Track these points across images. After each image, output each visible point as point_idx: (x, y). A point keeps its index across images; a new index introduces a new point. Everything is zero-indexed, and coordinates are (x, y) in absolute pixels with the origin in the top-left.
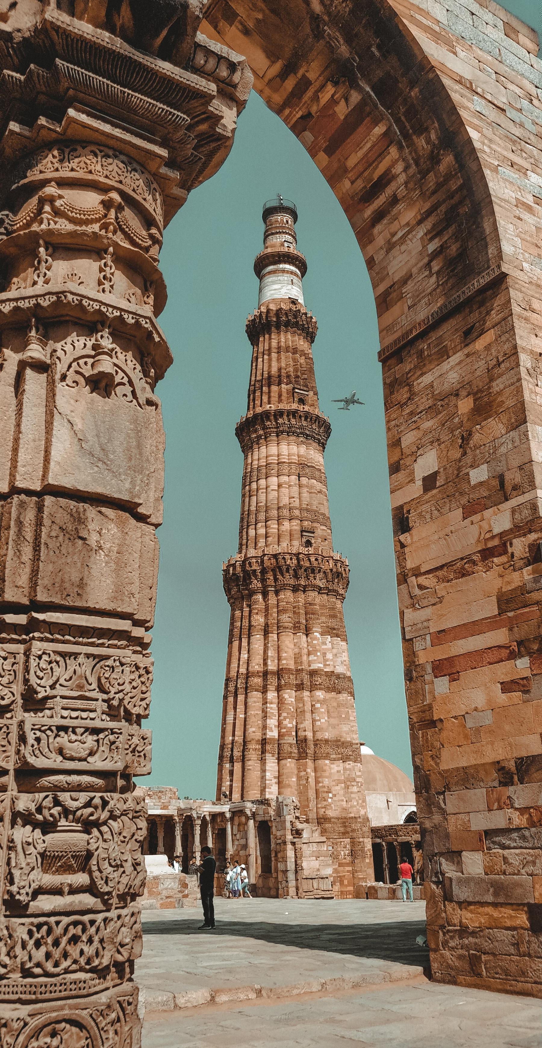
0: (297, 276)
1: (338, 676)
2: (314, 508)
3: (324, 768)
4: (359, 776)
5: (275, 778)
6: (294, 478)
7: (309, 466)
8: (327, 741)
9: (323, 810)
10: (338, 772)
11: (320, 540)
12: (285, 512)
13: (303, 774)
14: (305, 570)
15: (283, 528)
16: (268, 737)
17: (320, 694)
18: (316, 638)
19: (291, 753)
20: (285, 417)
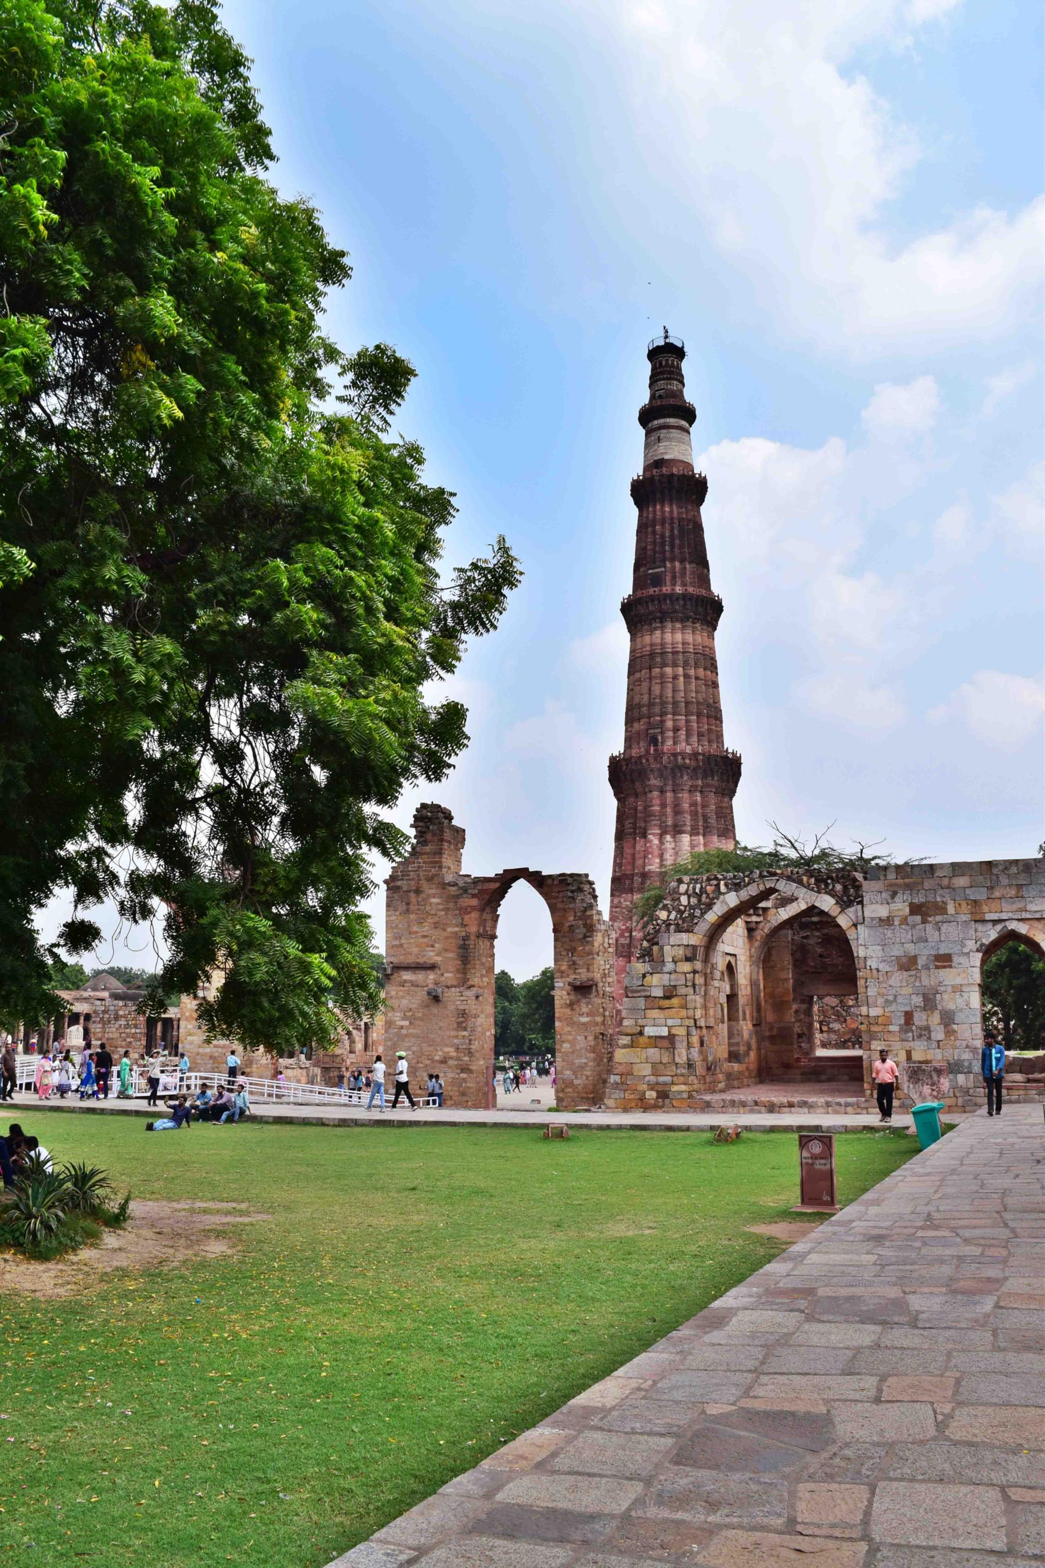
7: (661, 653)
11: (671, 734)
14: (640, 773)
18: (650, 841)
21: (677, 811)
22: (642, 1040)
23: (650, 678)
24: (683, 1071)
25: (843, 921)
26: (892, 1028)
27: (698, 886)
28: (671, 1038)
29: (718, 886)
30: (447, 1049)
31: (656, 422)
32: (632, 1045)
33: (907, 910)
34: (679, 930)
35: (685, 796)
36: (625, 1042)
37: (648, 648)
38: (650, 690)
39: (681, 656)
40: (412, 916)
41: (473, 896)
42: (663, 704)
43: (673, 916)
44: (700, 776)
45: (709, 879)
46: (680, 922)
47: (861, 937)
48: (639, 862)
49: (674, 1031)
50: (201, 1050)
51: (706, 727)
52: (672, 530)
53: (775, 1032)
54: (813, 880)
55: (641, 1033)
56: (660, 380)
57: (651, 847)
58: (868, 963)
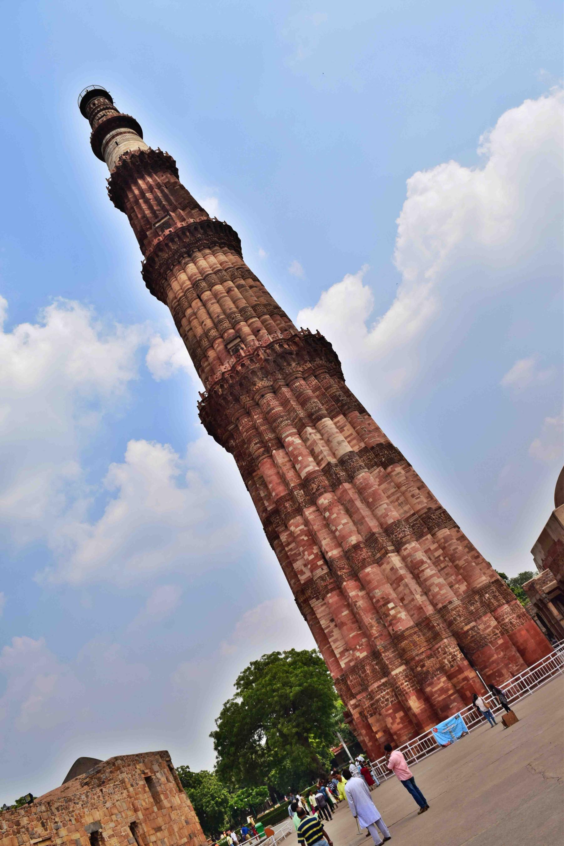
0: (121, 133)
1: (342, 462)
2: (228, 311)
3: (368, 578)
4: (436, 550)
5: (332, 620)
6: (196, 303)
7: (204, 279)
8: (356, 547)
9: (390, 628)
10: (392, 569)
11: (252, 337)
12: (205, 343)
13: (350, 600)
14: (241, 385)
15: (211, 359)
16: (302, 582)
17: (324, 500)
19: (326, 586)
20: (156, 259)
21: (303, 401)
23: (204, 305)
31: (109, 135)
35: (300, 383)
37: (188, 283)
38: (209, 313)
39: (224, 273)
42: (229, 316)
44: (307, 357)
48: (290, 475)
51: (283, 323)
52: (162, 191)
56: (99, 112)
57: (295, 449)
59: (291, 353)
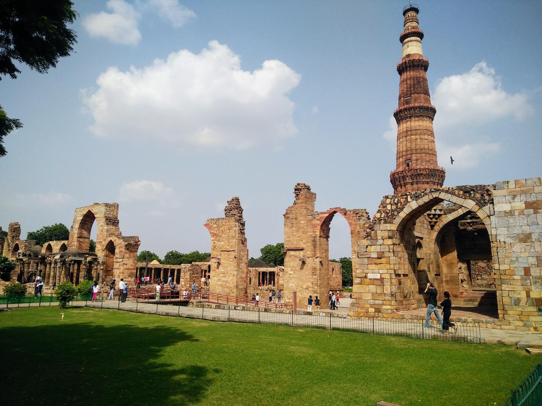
22: (366, 280)
24: (389, 298)
25: (481, 214)
26: (515, 277)
27: (396, 199)
28: (382, 279)
29: (406, 198)
30: (308, 284)
32: (360, 284)
33: (524, 206)
34: (385, 222)
36: (358, 281)
40: (294, 229)
41: (318, 220)
42: (411, 150)
43: (383, 216)
45: (402, 196)
46: (386, 218)
47: (493, 223)
49: (383, 276)
50: (217, 283)
52: (414, 82)
53: (448, 279)
54: (461, 192)
55: (366, 277)
58: (498, 238)
59: (422, 174)
